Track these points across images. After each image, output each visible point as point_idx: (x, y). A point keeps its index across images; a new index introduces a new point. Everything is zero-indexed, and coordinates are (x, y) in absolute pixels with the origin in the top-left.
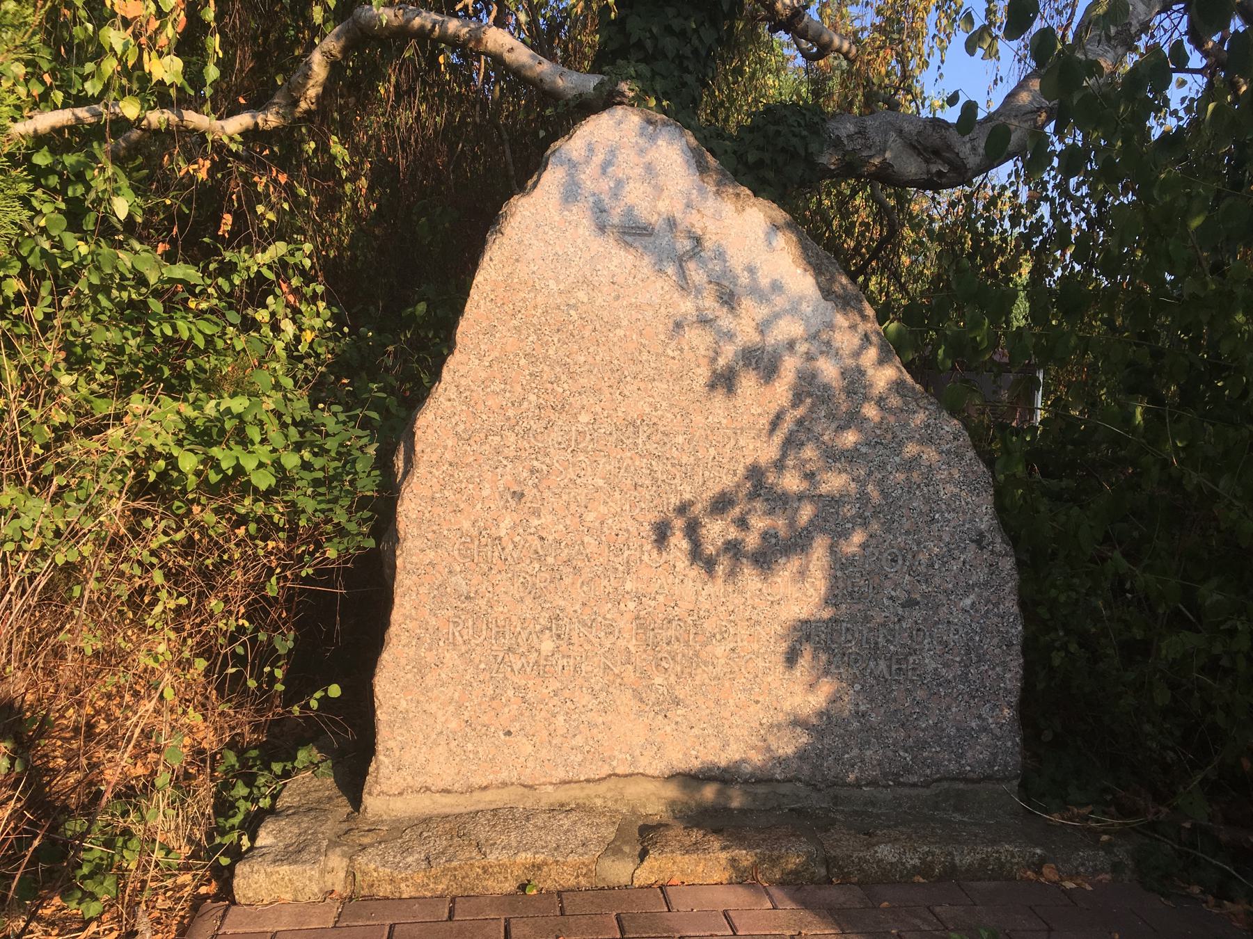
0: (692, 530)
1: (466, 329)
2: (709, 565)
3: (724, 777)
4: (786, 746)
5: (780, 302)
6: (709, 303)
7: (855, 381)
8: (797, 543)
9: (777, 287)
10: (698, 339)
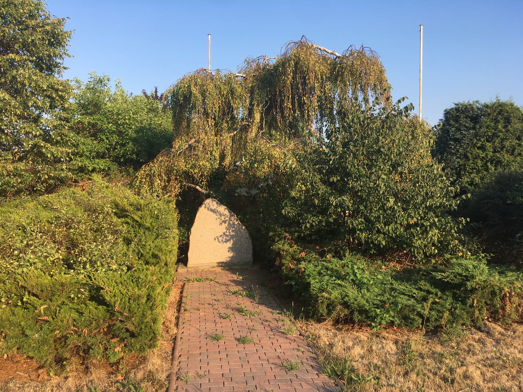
0: (218, 239)
1: (195, 220)
2: (220, 242)
3: (222, 263)
4: (228, 260)
5: (226, 216)
6: (219, 216)
7: (234, 223)
8: (229, 240)
9: (225, 215)
10: (218, 220)
